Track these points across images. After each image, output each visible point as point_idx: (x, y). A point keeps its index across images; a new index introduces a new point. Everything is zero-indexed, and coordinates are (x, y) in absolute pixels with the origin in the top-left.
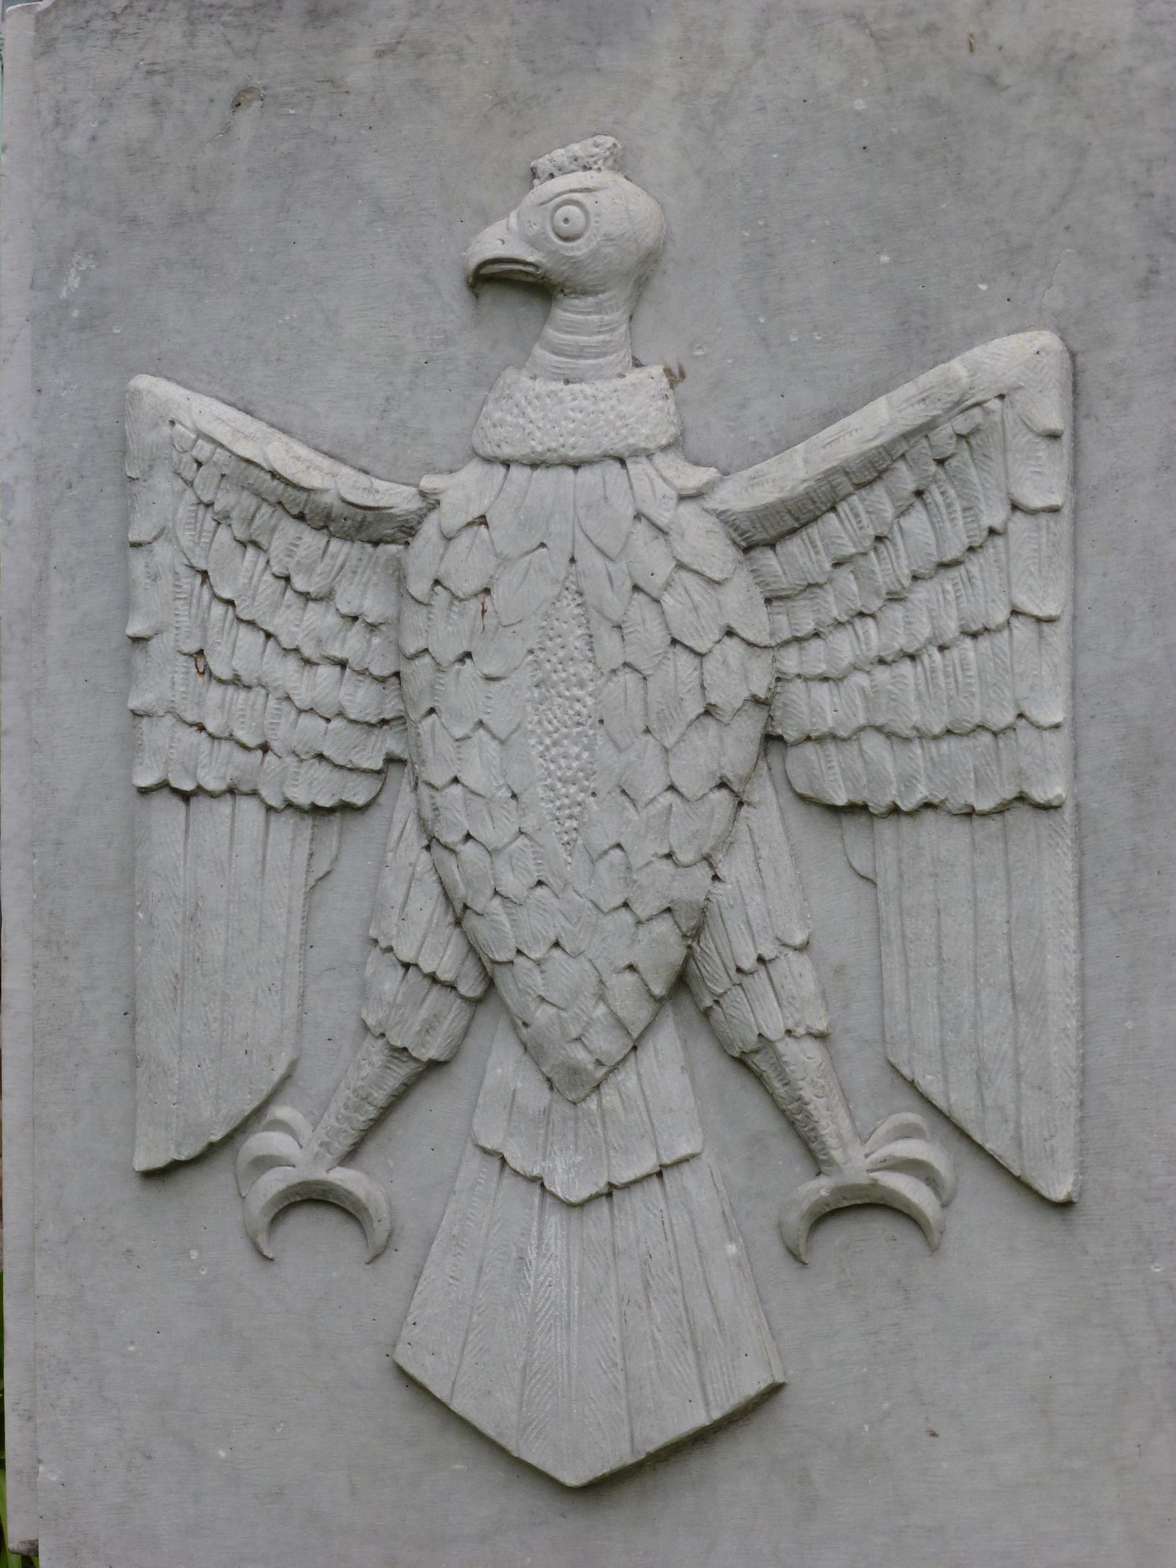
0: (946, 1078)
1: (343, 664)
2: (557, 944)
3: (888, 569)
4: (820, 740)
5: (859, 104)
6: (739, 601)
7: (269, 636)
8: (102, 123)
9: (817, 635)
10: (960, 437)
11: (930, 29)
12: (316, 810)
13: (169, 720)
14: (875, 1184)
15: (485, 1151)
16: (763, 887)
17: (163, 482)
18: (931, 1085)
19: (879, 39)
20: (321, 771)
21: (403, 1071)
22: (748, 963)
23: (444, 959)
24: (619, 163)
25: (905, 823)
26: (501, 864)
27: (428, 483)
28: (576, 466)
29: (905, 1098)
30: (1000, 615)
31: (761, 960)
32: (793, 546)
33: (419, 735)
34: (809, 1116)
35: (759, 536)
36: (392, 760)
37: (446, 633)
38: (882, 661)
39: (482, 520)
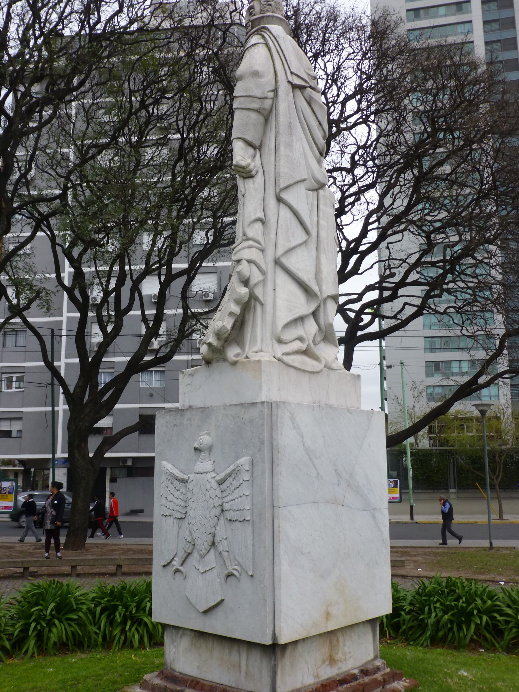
3: (232, 488)
6: (218, 492)
20: (179, 513)
21: (186, 554)
24: (208, 434)
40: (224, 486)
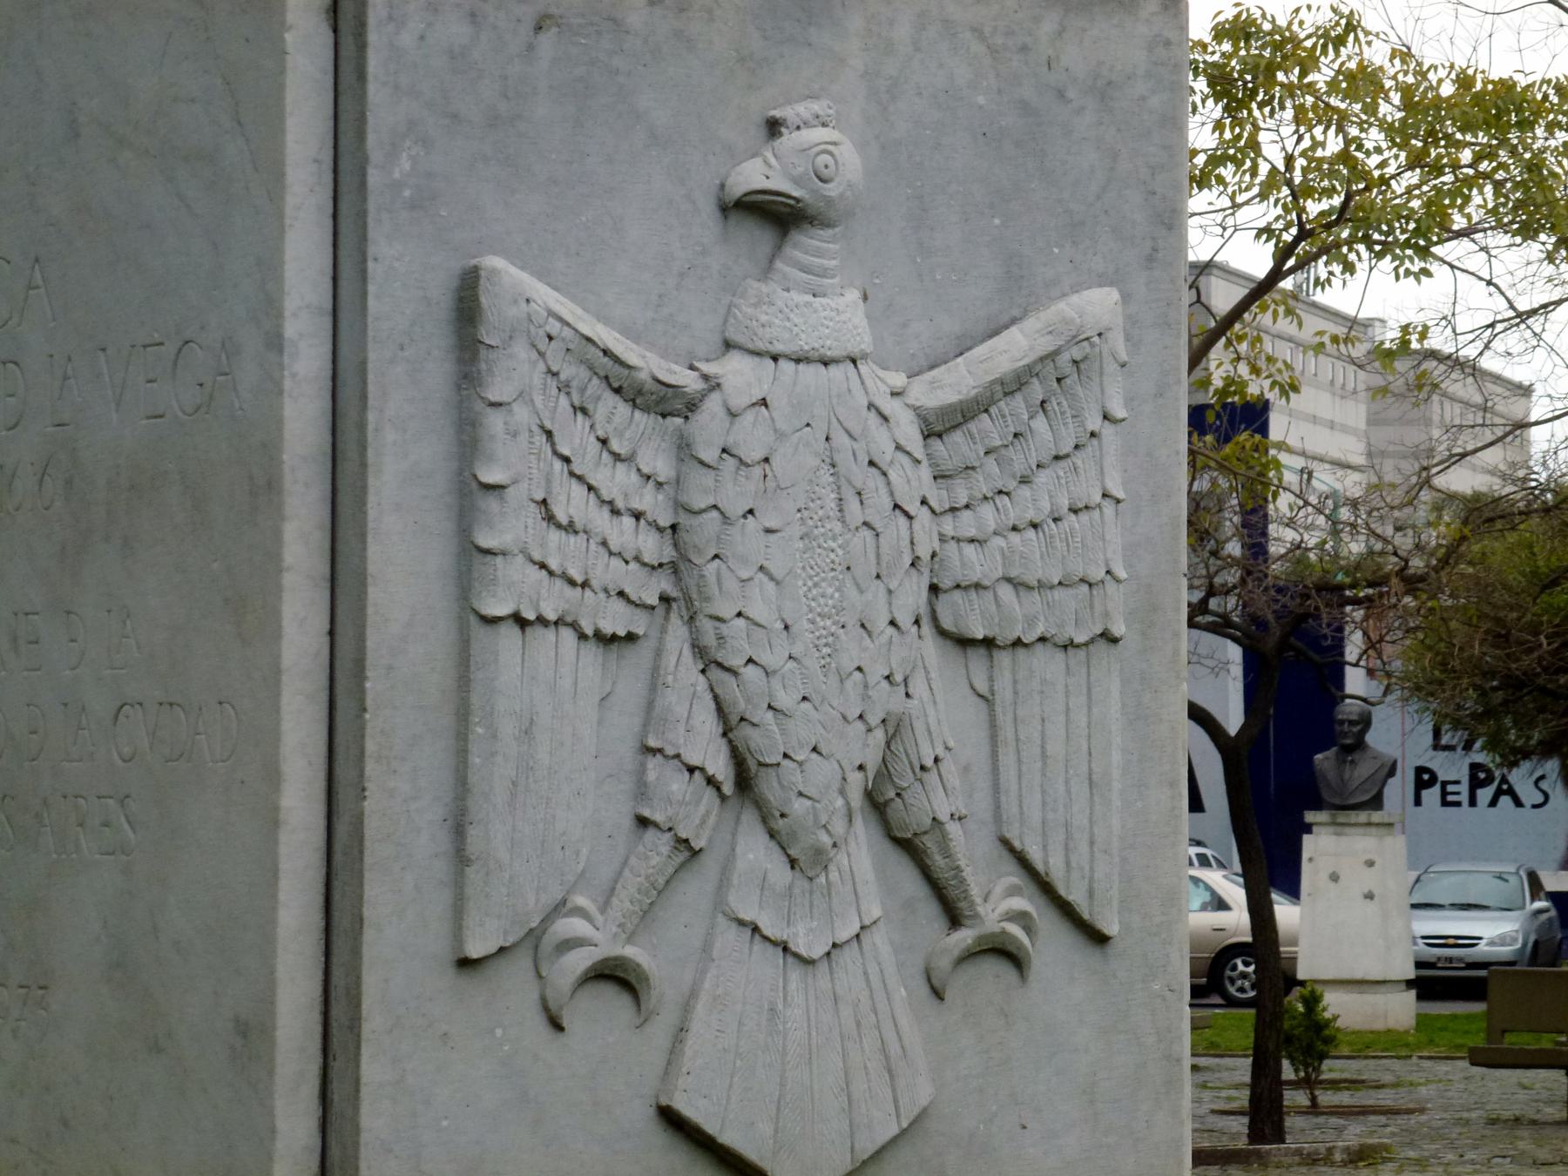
0: (1045, 847)
1: (638, 516)
2: (814, 749)
3: (1019, 460)
4: (966, 588)
5: (981, 100)
7: (590, 488)
8: (429, 25)
9: (967, 506)
10: (1075, 362)
11: (1024, 49)
12: (614, 638)
13: (520, 559)
14: (1004, 932)
15: (741, 923)
16: (935, 703)
17: (521, 351)
18: (1035, 855)
19: (993, 51)
20: (618, 605)
22: (929, 763)
23: (720, 766)
25: (1021, 651)
26: (776, 683)
27: (706, 368)
28: (825, 363)
29: (1010, 865)
30: (1097, 498)
31: (936, 760)
32: (957, 437)
33: (703, 576)
34: (963, 881)
35: (938, 428)
36: (665, 599)
37: (735, 492)
38: (1014, 529)
39: (764, 402)
40: (957, 448)
